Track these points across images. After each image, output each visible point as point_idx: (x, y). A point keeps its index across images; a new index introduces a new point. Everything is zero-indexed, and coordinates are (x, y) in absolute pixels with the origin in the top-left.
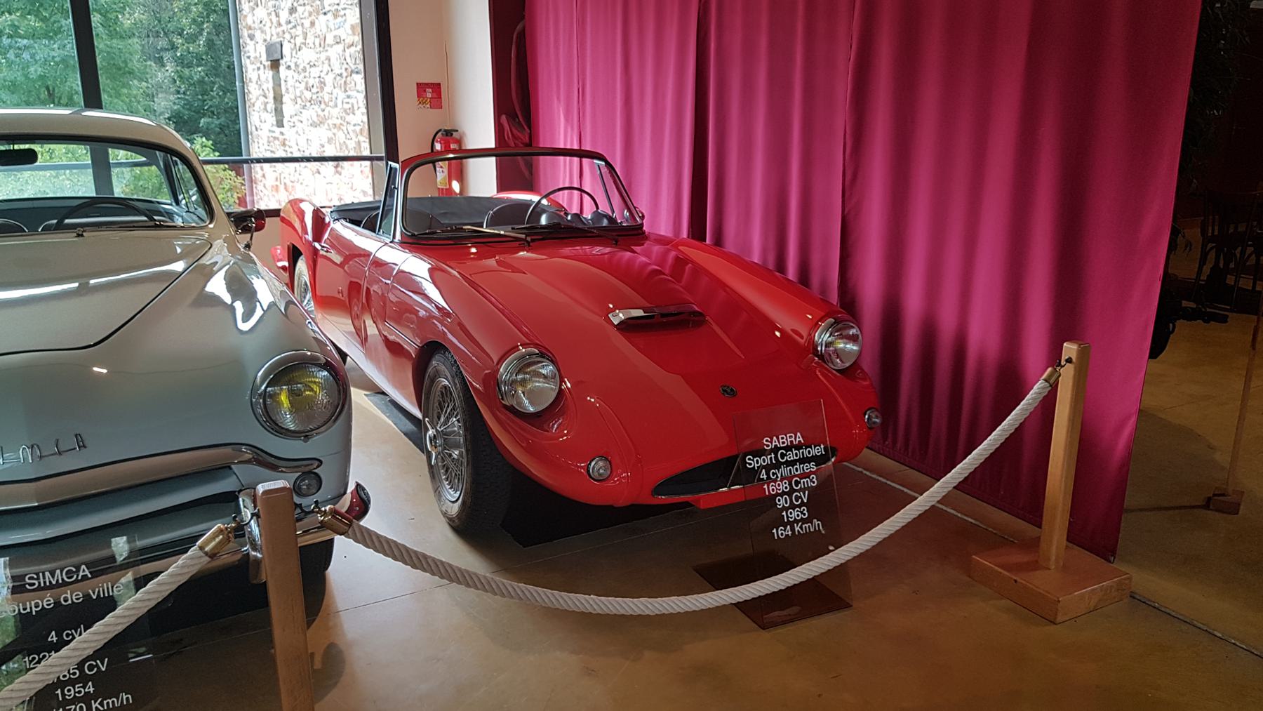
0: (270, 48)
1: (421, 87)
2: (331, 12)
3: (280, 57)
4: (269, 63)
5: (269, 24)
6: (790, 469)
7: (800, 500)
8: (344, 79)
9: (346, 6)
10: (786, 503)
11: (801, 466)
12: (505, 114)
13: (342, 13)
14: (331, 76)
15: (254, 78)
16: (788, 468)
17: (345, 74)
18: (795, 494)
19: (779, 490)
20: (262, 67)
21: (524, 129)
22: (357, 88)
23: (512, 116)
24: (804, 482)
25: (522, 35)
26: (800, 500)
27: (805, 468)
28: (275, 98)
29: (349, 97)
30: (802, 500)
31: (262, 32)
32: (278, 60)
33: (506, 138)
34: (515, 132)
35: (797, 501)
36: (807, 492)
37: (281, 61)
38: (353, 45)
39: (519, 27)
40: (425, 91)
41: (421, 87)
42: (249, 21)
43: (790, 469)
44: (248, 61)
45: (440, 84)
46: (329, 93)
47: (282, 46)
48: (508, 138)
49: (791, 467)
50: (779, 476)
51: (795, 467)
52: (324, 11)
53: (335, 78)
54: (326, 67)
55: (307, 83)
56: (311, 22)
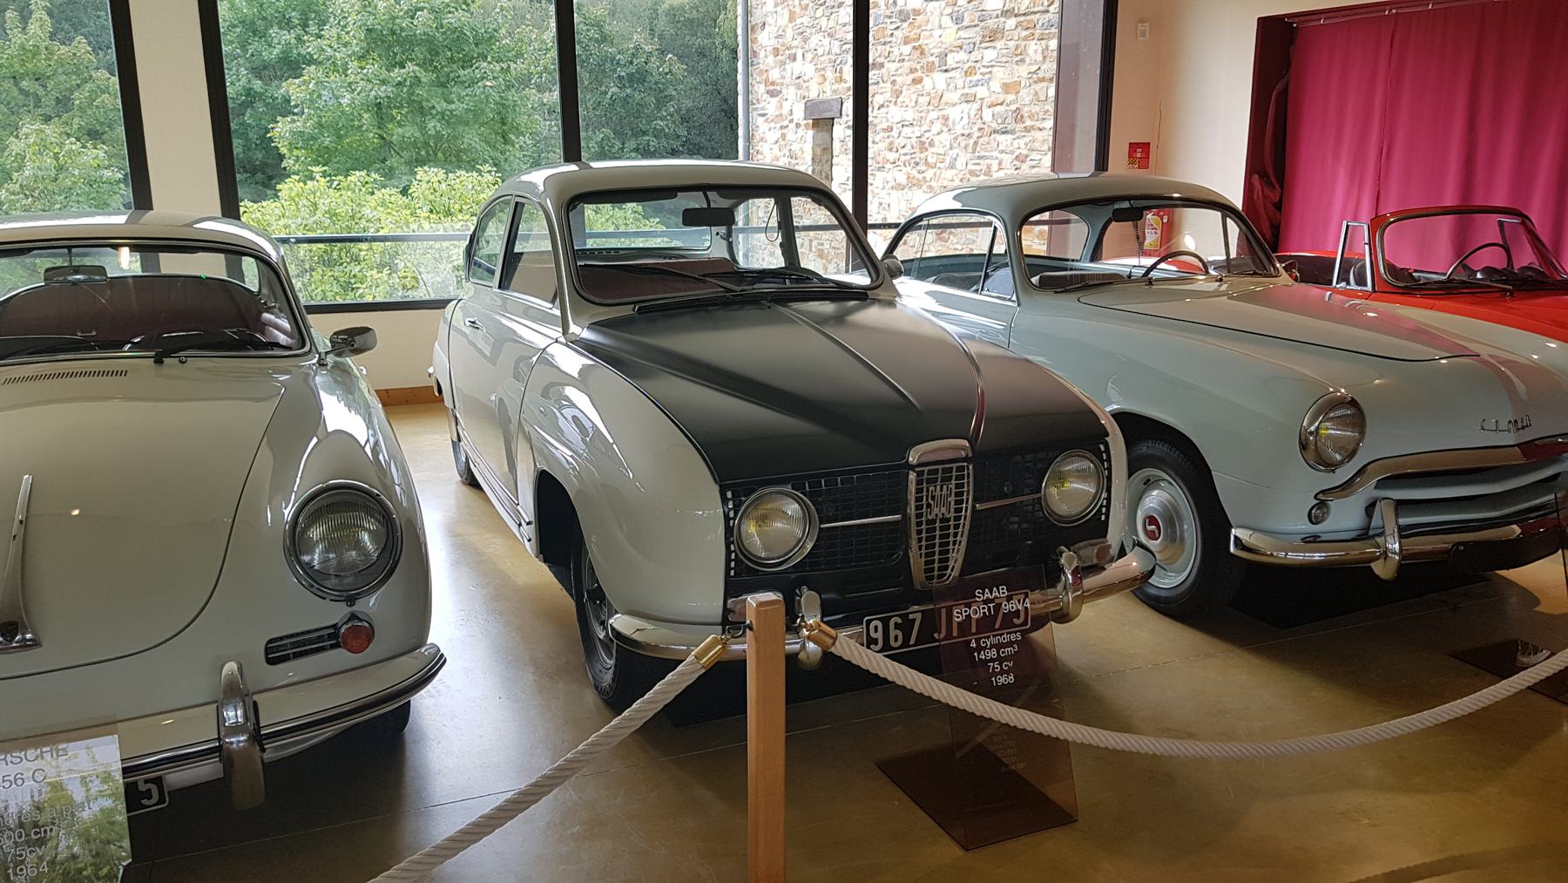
0: (810, 107)
1: (1133, 147)
2: (959, 70)
3: (838, 115)
4: (811, 121)
5: (817, 79)
8: (974, 139)
9: (993, 63)
12: (1257, 173)
13: (984, 70)
14: (946, 138)
15: (773, 136)
17: (977, 134)
20: (792, 126)
21: (1275, 188)
22: (1001, 147)
23: (1263, 176)
25: (1284, 93)
28: (813, 159)
29: (980, 158)
31: (799, 87)
32: (833, 119)
33: (1255, 197)
34: (1266, 190)
37: (835, 120)
38: (1001, 104)
39: (1280, 86)
40: (1135, 151)
41: (1133, 147)
42: (775, 75)
44: (760, 120)
45: (1149, 144)
46: (940, 154)
47: (842, 103)
48: (1258, 197)
52: (944, 68)
53: (956, 139)
54: (937, 127)
55: (891, 143)
56: (913, 80)
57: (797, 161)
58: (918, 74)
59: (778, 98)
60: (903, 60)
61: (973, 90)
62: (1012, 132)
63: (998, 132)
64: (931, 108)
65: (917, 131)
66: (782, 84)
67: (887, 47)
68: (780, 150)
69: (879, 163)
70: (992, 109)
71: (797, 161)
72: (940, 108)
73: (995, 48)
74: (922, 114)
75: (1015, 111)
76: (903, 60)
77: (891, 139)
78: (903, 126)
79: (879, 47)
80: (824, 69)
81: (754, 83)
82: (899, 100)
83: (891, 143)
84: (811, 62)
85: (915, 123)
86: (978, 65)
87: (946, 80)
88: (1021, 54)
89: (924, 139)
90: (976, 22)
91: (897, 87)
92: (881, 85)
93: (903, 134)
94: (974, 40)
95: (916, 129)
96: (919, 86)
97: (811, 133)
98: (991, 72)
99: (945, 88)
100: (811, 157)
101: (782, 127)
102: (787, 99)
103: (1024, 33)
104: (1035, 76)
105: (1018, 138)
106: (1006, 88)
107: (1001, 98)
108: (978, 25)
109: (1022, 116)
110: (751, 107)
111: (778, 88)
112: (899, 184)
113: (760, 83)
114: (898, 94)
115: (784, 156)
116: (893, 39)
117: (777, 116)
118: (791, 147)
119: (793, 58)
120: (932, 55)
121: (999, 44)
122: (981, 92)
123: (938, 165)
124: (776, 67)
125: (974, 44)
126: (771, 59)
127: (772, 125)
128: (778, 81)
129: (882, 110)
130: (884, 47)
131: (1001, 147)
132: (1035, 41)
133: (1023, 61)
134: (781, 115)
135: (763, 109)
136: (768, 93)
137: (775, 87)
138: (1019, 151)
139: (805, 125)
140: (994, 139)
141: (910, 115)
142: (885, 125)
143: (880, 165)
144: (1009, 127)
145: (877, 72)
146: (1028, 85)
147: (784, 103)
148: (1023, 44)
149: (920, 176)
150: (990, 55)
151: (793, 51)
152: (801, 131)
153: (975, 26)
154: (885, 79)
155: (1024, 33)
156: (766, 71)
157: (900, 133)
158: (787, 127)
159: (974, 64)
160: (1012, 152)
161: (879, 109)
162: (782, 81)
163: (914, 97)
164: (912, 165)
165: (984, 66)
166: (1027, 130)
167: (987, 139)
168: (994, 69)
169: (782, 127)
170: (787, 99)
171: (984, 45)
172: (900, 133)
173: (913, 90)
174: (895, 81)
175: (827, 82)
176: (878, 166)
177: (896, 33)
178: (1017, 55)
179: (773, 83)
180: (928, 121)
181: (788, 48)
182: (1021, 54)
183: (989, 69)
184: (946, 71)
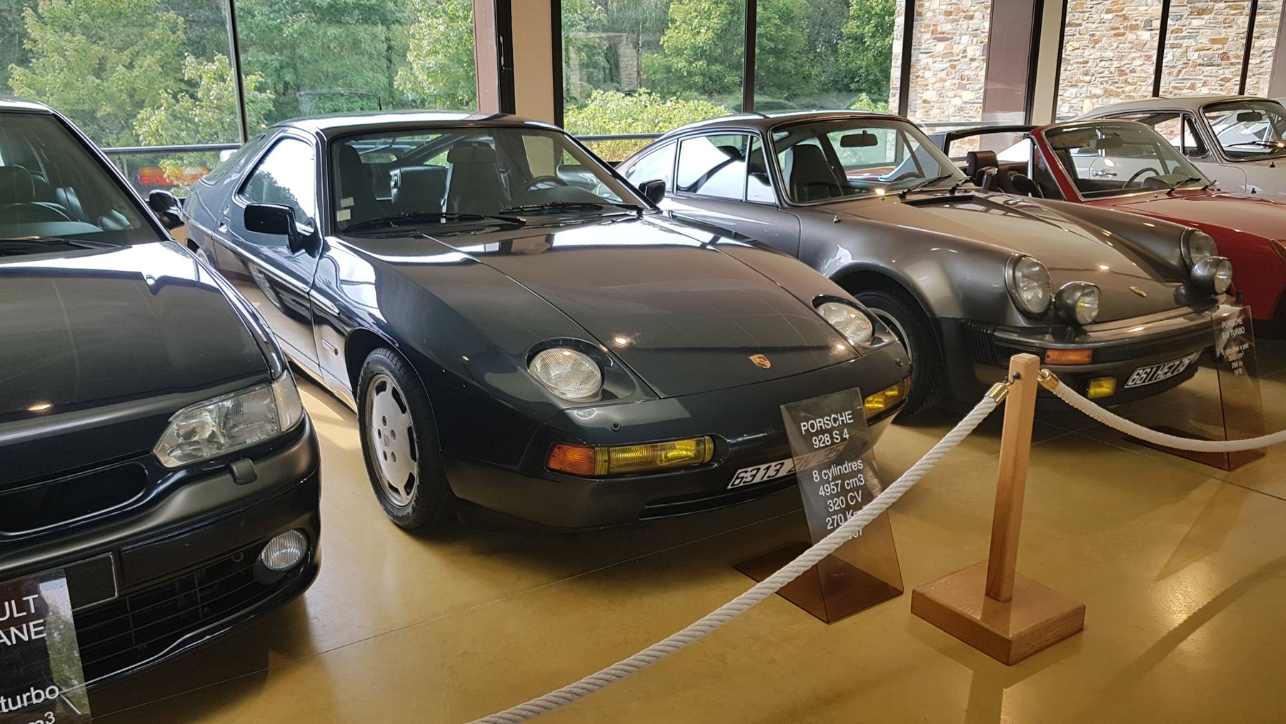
6: (840, 469)
7: (855, 501)
8: (1178, 68)
10: (843, 505)
11: (850, 465)
16: (838, 468)
18: (850, 494)
19: (828, 492)
24: (853, 482)
26: (855, 501)
27: (853, 466)
30: (857, 500)
35: (852, 501)
36: (860, 492)
43: (840, 469)
49: (840, 467)
50: (831, 476)
51: (844, 466)
52: (1149, 28)
57: (970, 82)
58: (1122, 31)
59: (949, 42)
60: (1104, 23)
61: (1182, 41)
62: (1218, 65)
63: (1203, 65)
64: (1132, 50)
65: (1116, 64)
66: (955, 34)
67: (1087, 15)
68: (947, 75)
69: (1071, 82)
70: (1198, 52)
71: (970, 82)
72: (1144, 50)
73: (1202, 19)
74: (1124, 54)
75: (1221, 54)
76: (1104, 23)
77: (1087, 68)
78: (1101, 61)
79: (1077, 14)
82: (1097, 46)
83: (1087, 70)
85: (1114, 59)
86: (1184, 28)
87: (1151, 35)
88: (1229, 23)
89: (1123, 68)
90: (1185, 4)
91: (1096, 38)
92: (1078, 36)
93: (1100, 65)
94: (1182, 14)
95: (1116, 62)
96: (1120, 38)
98: (1198, 32)
99: (1149, 39)
101: (951, 61)
102: (959, 43)
103: (1233, 12)
104: (1241, 35)
105: (1223, 68)
106: (1214, 41)
107: (1209, 46)
108: (1186, 6)
109: (1228, 57)
111: (949, 36)
112: (1095, 95)
113: (924, 32)
114: (1096, 42)
115: (953, 78)
116: (1093, 9)
117: (946, 54)
118: (963, 73)
119: (972, 18)
120: (1136, 20)
121: (1207, 17)
122: (1185, 43)
123: (1139, 83)
124: (947, 23)
125: (1182, 16)
126: (942, 17)
127: (940, 59)
128: (949, 31)
129: (1075, 51)
130: (1082, 14)
131: (1205, 74)
132: (1243, 17)
133: (1230, 27)
134: (952, 53)
135: (925, 49)
136: (934, 39)
137: (945, 35)
138: (1223, 76)
140: (1200, 69)
141: (1109, 54)
142: (1081, 60)
143: (1074, 83)
144: (1214, 63)
145: (1074, 29)
146: (1235, 39)
147: (955, 46)
148: (1232, 17)
149: (1120, 90)
150: (1196, 23)
151: (971, 13)
152: (975, 64)
153: (1184, 6)
154: (1082, 33)
155: (1233, 12)
156: (934, 25)
157: (1097, 65)
158: (959, 60)
159: (1180, 27)
160: (1215, 77)
161: (1073, 50)
162: (955, 31)
163: (1115, 45)
164: (1110, 83)
165: (1191, 29)
166: (1232, 64)
167: (1191, 69)
168: (1201, 31)
169: (951, 61)
170: (959, 43)
171: (1191, 17)
172: (1097, 65)
173: (1113, 39)
174: (1093, 34)
176: (1069, 84)
177: (1095, 6)
178: (1224, 23)
179: (943, 33)
180: (1129, 58)
181: (964, 12)
182: (1229, 23)
183: (1197, 30)
184: (1151, 30)
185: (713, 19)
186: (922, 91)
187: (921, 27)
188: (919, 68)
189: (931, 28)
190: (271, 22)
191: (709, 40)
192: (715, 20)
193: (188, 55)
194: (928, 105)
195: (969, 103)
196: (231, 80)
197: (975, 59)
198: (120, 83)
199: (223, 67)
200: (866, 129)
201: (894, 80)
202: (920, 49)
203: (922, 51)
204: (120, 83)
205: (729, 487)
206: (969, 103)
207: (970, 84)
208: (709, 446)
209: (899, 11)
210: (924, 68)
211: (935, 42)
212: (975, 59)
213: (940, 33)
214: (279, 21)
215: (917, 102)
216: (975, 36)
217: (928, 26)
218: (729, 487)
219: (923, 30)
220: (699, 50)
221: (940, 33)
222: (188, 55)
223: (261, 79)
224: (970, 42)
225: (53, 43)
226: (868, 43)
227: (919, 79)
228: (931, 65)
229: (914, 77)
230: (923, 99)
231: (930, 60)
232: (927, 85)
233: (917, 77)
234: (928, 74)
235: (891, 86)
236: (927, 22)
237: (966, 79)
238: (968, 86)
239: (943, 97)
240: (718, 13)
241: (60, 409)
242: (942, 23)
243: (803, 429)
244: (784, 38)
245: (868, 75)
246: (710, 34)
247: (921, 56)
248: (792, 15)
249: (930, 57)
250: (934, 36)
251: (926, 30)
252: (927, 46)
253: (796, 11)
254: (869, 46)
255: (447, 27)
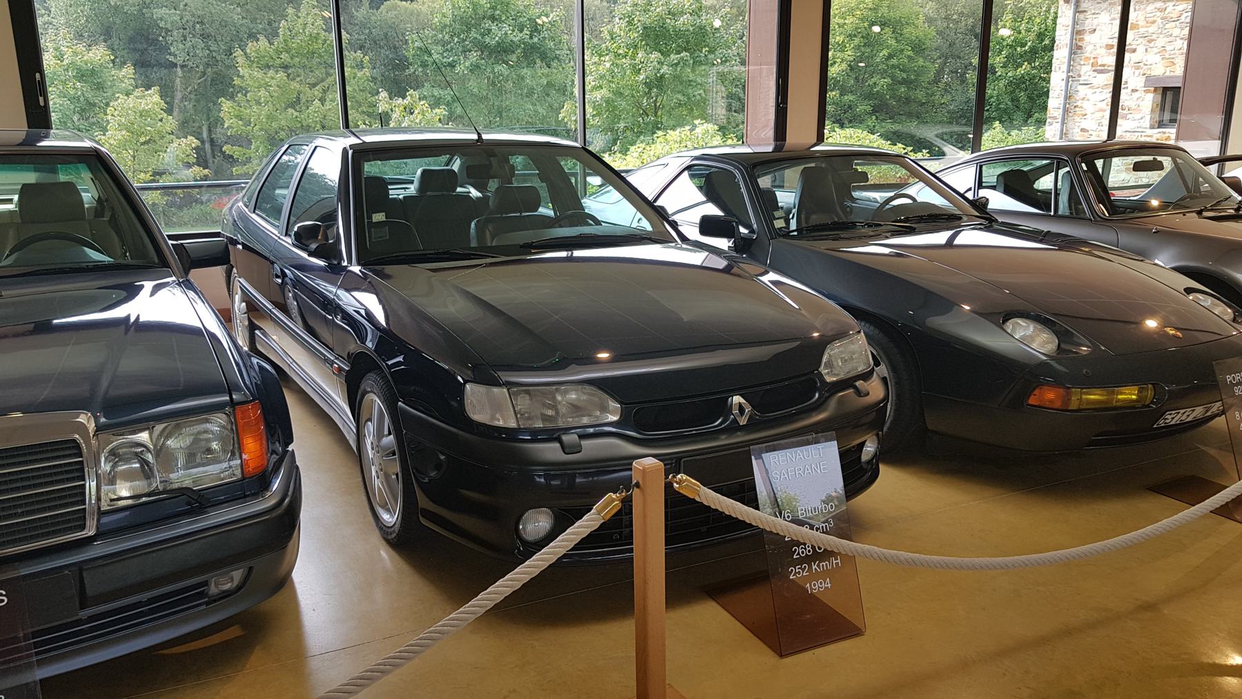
0: (1149, 80)
57: (1130, 112)
71: (1130, 112)
80: (1173, 58)
81: (1075, 64)
84: (1156, 54)
97: (1150, 96)
100: (1150, 110)
110: (1070, 79)
113: (1084, 65)
126: (1103, 51)
127: (1100, 90)
135: (1085, 80)
136: (1094, 71)
137: (1106, 68)
139: (1145, 91)
152: (1136, 95)
156: (1094, 58)
175: (1178, 65)
179: (1104, 65)
185: (847, 51)
186: (1080, 121)
187: (1081, 60)
188: (1078, 98)
189: (1092, 61)
190: (445, 60)
191: (843, 71)
192: (849, 53)
193: (382, 91)
194: (1086, 134)
195: (1130, 132)
196: (419, 113)
197: (1137, 90)
198: (316, 115)
199: (414, 101)
200: (1157, 157)
201: (1051, 110)
202: (1079, 80)
203: (1081, 82)
204: (316, 115)
205: (1155, 426)
206: (1130, 132)
207: (1131, 113)
208: (1150, 393)
209: (1058, 45)
210: (1083, 99)
211: (1095, 74)
212: (1137, 90)
213: (1100, 66)
214: (451, 59)
215: (1074, 131)
216: (1138, 68)
217: (1088, 58)
218: (1155, 426)
219: (1082, 62)
220: (833, 81)
221: (1100, 66)
222: (382, 91)
223: (444, 113)
224: (1132, 74)
225: (259, 80)
226: (999, 73)
227: (1077, 109)
228: (1090, 96)
229: (1072, 107)
230: (1080, 128)
231: (1091, 91)
232: (1086, 115)
233: (1075, 107)
234: (1085, 104)
235: (1048, 115)
236: (1087, 55)
237: (1127, 109)
238: (1129, 116)
239: (1102, 126)
240: (852, 46)
241: (615, 360)
242: (1102, 57)
243: (1228, 380)
244: (916, 68)
245: (999, 104)
246: (844, 66)
247: (1080, 88)
248: (923, 47)
249: (1090, 88)
250: (1094, 69)
251: (1085, 63)
252: (1085, 78)
253: (928, 43)
254: (1000, 76)
255: (612, 64)
